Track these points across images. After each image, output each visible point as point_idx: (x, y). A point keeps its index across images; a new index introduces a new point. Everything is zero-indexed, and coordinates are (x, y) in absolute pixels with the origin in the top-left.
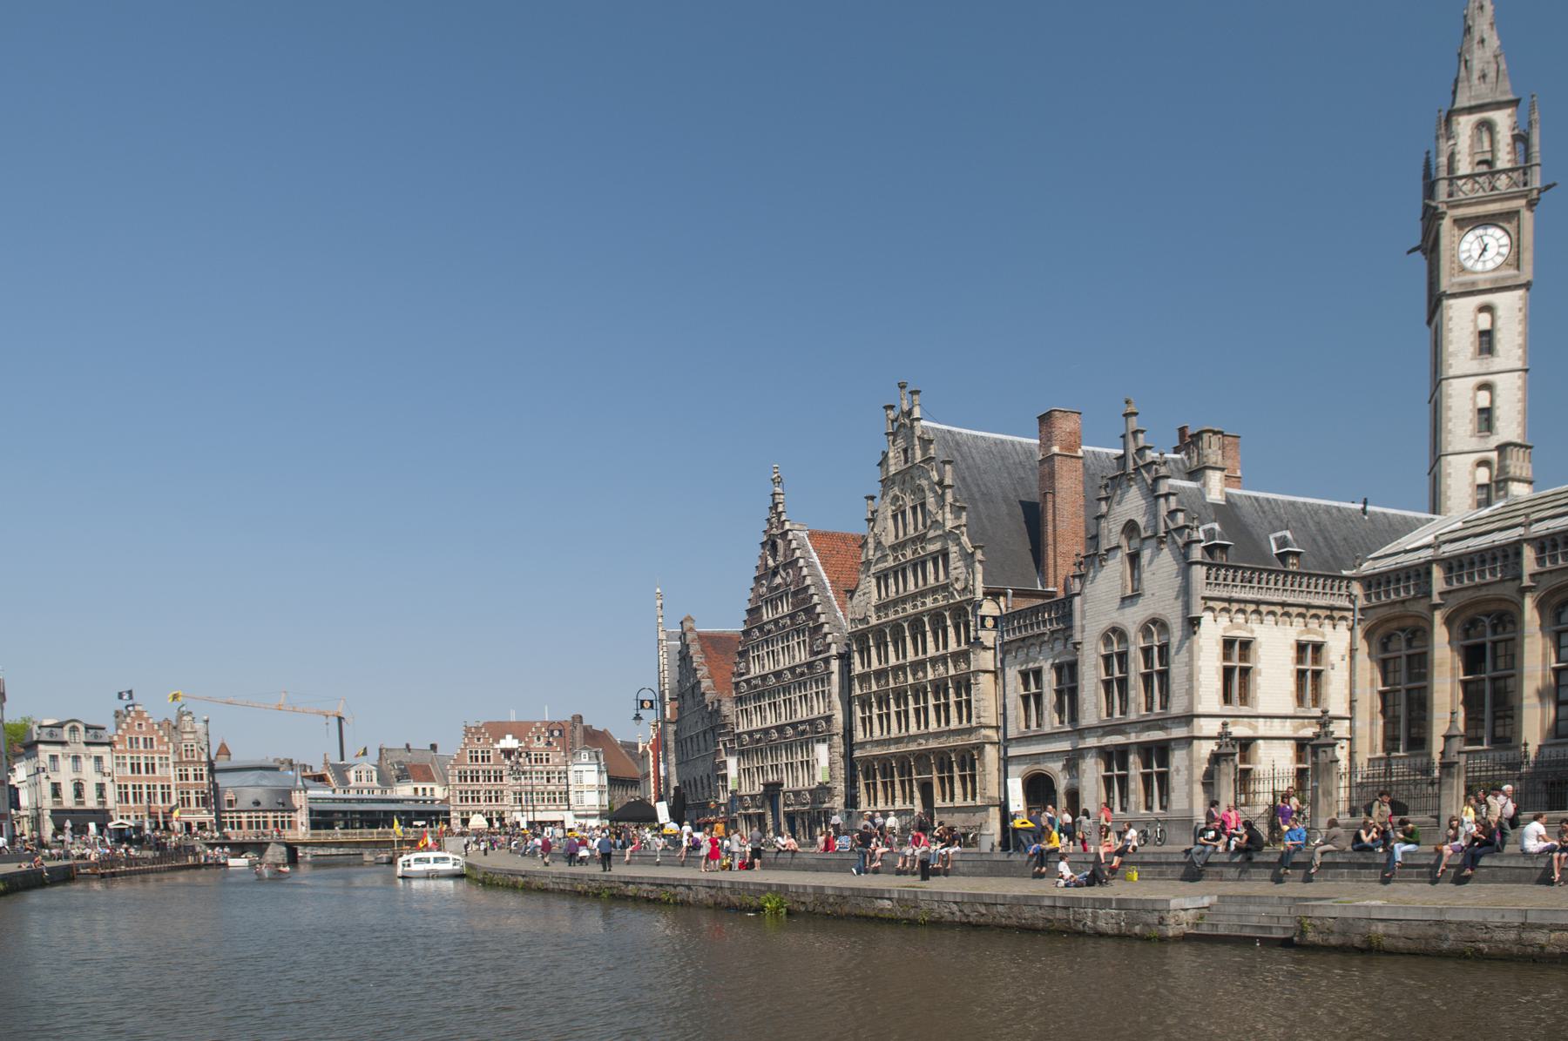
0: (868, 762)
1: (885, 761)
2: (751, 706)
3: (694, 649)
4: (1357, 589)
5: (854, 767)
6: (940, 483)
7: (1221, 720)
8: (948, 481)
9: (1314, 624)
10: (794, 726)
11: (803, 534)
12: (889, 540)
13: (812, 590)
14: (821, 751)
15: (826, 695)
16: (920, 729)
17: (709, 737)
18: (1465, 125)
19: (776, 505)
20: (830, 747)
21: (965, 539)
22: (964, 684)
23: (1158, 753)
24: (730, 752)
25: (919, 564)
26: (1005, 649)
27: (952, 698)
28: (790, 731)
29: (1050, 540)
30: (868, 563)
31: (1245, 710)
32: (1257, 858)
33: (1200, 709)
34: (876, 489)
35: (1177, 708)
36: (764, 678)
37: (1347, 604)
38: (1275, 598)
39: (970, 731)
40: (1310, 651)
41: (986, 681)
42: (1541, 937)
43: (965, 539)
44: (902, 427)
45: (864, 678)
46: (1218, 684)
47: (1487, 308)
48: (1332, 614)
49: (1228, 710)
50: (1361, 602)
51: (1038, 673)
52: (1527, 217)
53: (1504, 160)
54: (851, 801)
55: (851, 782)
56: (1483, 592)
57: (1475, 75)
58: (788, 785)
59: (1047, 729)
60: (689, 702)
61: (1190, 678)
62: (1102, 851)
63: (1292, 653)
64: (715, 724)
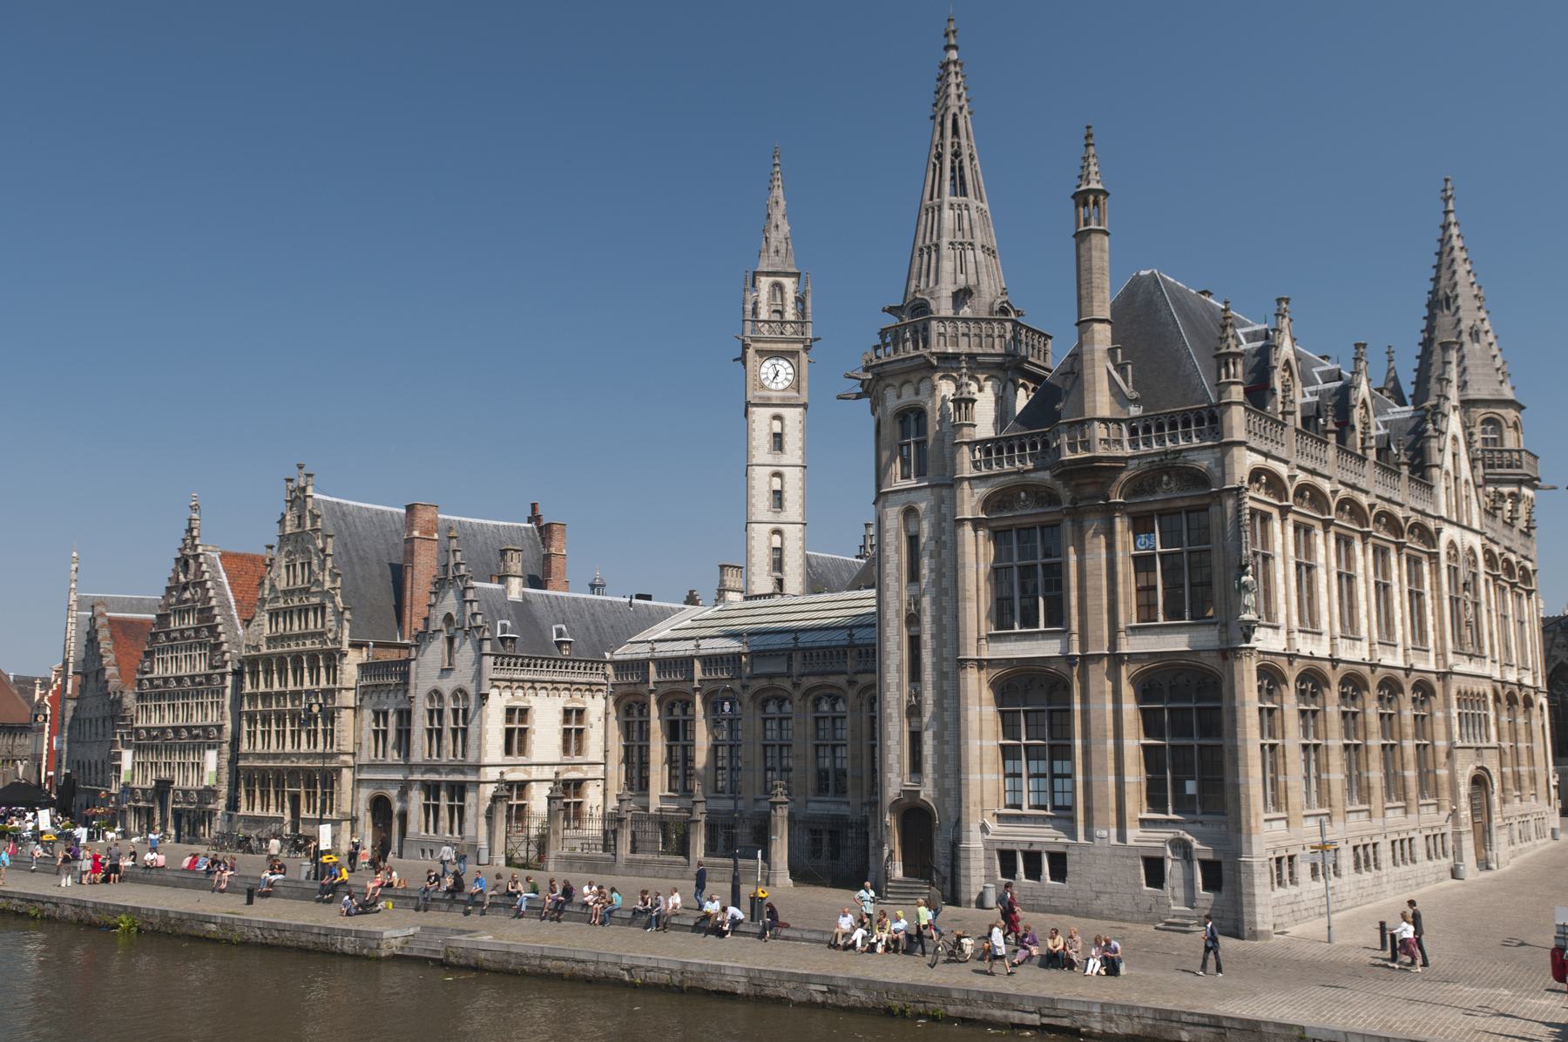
0: (250, 771)
1: (264, 771)
2: (151, 704)
3: (103, 634)
4: (610, 670)
6: (323, 550)
7: (500, 769)
8: (329, 551)
9: (577, 695)
10: (189, 729)
11: (216, 555)
12: (282, 585)
13: (216, 611)
14: (211, 758)
15: (220, 706)
16: (293, 747)
18: (765, 283)
19: (190, 530)
20: (219, 754)
21: (338, 599)
22: (330, 716)
23: (458, 790)
24: (127, 745)
25: (303, 611)
26: (364, 691)
27: (320, 727)
28: (185, 734)
29: (408, 602)
30: (263, 601)
31: (522, 760)
32: (459, 897)
33: (486, 761)
34: (275, 541)
36: (166, 680)
37: (603, 680)
38: (547, 678)
39: (332, 756)
41: (347, 716)
42: (548, 964)
43: (338, 599)
44: (298, 499)
45: (253, 697)
46: (501, 741)
47: (778, 417)
48: (591, 688)
50: (612, 679)
51: (386, 714)
52: (803, 355)
53: (790, 314)
54: (233, 805)
56: (676, 686)
57: (772, 250)
58: (178, 783)
59: (389, 761)
61: (480, 737)
62: (371, 885)
63: (560, 717)
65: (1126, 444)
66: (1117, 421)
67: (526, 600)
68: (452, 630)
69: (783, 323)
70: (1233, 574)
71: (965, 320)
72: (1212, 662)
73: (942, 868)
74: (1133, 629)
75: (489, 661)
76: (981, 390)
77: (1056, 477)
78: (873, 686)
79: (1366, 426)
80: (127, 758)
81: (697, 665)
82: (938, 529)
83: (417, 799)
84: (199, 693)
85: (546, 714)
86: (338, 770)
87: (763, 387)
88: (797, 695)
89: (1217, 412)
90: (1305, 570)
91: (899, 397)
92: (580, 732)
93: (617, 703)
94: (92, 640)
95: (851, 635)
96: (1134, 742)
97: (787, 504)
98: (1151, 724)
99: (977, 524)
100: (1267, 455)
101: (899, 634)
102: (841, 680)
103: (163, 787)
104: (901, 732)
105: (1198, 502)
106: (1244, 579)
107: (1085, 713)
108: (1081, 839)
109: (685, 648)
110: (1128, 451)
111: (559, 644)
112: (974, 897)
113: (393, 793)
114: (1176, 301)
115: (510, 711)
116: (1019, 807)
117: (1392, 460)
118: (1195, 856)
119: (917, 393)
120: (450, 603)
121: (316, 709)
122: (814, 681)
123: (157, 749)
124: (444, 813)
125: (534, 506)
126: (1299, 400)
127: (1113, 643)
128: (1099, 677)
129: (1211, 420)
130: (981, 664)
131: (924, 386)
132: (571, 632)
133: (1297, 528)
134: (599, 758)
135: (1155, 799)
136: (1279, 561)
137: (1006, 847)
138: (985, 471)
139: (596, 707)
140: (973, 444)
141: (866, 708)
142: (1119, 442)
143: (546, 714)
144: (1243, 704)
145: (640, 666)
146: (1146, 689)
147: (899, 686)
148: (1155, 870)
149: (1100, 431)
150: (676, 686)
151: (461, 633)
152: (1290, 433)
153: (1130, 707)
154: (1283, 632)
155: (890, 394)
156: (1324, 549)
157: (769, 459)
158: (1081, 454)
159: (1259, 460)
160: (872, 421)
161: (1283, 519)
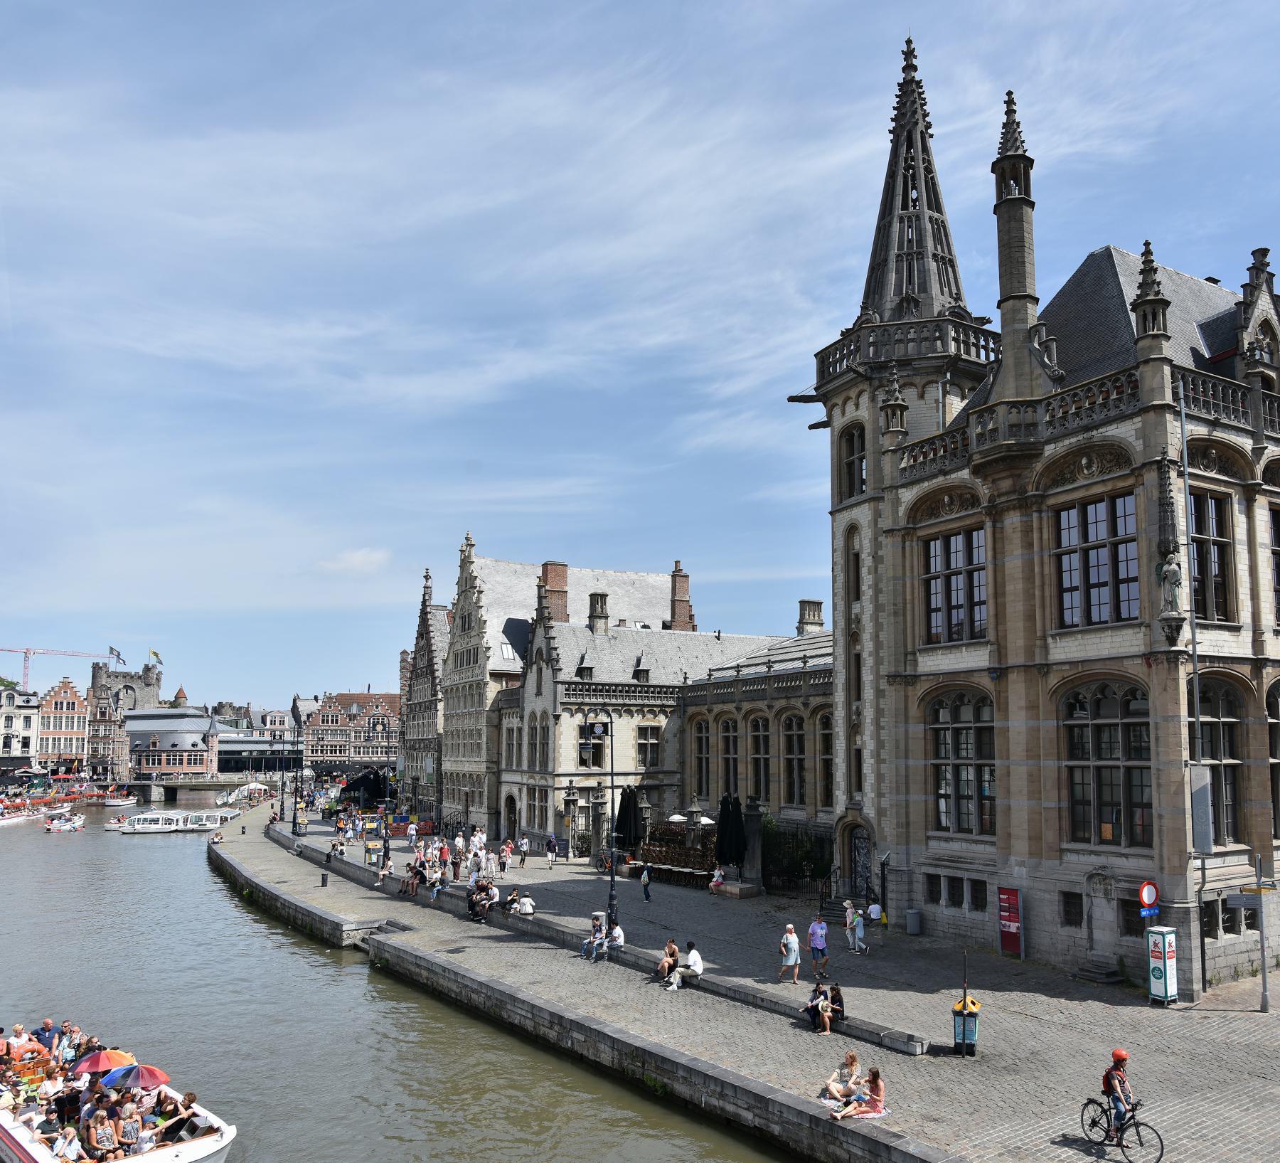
31: (595, 769)
33: (560, 771)
63: (635, 734)
72: (1136, 669)
76: (922, 396)
82: (877, 545)
91: (843, 414)
99: (907, 533)
105: (1121, 484)
106: (1166, 568)
113: (515, 790)
115: (586, 731)
122: (783, 703)
128: (1017, 689)
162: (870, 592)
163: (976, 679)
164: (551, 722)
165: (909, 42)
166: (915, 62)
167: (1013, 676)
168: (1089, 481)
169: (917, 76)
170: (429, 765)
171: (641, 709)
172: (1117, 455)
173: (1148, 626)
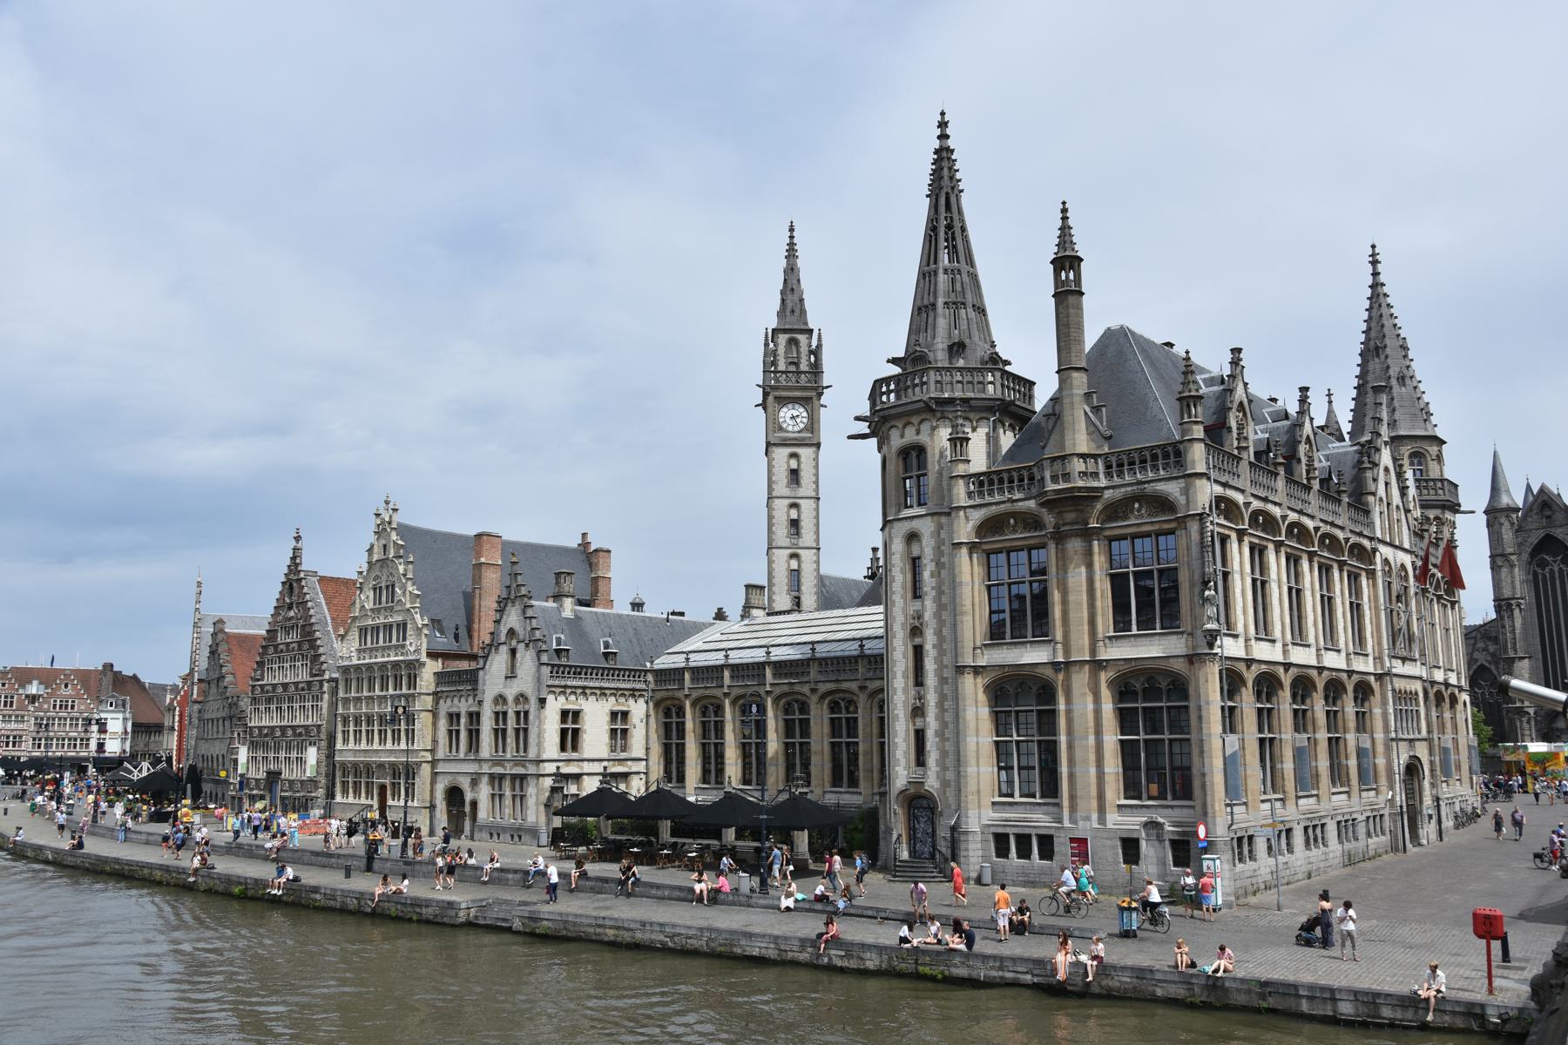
1: (355, 765)
2: (262, 708)
4: (650, 678)
5: (330, 764)
9: (622, 700)
10: (293, 728)
17: (227, 723)
22: (411, 719)
28: (290, 732)
31: (575, 755)
33: (545, 757)
34: (365, 567)
35: (532, 754)
36: (274, 686)
38: (597, 684)
40: (620, 716)
45: (346, 701)
46: (557, 740)
47: (794, 455)
48: (634, 694)
49: (564, 756)
50: (652, 686)
51: (458, 715)
55: (331, 777)
60: (214, 690)
61: (539, 735)
63: (608, 718)
64: (235, 717)
65: (1102, 476)
66: (1095, 457)
67: (578, 618)
68: (514, 643)
69: (799, 373)
70: (1197, 590)
71: (960, 369)
72: (1179, 666)
73: (944, 850)
74: (1110, 638)
75: (546, 670)
77: (1042, 505)
78: (882, 690)
79: (1311, 459)
80: (243, 754)
81: (727, 674)
82: (938, 551)
83: (484, 792)
84: (302, 698)
85: (596, 716)
86: (419, 764)
87: (781, 429)
88: (814, 699)
89: (1181, 447)
90: (1260, 587)
91: (902, 436)
92: (624, 731)
93: (657, 705)
94: (213, 653)
95: (862, 646)
96: (1111, 739)
97: (803, 531)
98: (1126, 720)
99: (972, 547)
100: (1225, 485)
101: (905, 644)
102: (854, 686)
103: (273, 776)
104: (907, 730)
105: (1166, 526)
107: (1069, 712)
108: (1067, 824)
109: (716, 659)
110: (1103, 482)
111: (606, 655)
112: (974, 875)
113: (465, 783)
114: (1143, 351)
115: (564, 714)
116: (1012, 795)
117: (1334, 488)
118: (1167, 837)
119: (918, 432)
120: (513, 618)
121: (400, 710)
123: (266, 747)
124: (508, 801)
125: (584, 535)
126: (1252, 437)
127: (1093, 651)
128: (1081, 679)
129: (1173, 455)
130: (977, 670)
131: (925, 427)
132: (617, 643)
133: (1252, 548)
134: (642, 754)
135: (1132, 788)
136: (1237, 577)
137: (1000, 830)
138: (978, 501)
139: (638, 709)
140: (967, 477)
141: (876, 710)
142: (1095, 475)
143: (596, 716)
144: (1208, 703)
145: (674, 675)
146: (1123, 690)
147: (905, 690)
148: (1130, 848)
149: (1078, 466)
150: (708, 692)
151: (521, 647)
152: (1244, 465)
153: (1108, 707)
154: (1241, 640)
155: (894, 435)
156: (1276, 564)
157: (786, 492)
158: (1062, 486)
159: (1218, 490)
160: (877, 458)
161: (1240, 541)
162: (934, 593)
163: (1040, 670)
164: (533, 706)
165: (943, 114)
166: (948, 131)
167: (1073, 669)
168: (1139, 520)
169: (951, 143)
170: (312, 755)
171: (616, 692)
172: (1163, 504)
173: (1191, 634)
